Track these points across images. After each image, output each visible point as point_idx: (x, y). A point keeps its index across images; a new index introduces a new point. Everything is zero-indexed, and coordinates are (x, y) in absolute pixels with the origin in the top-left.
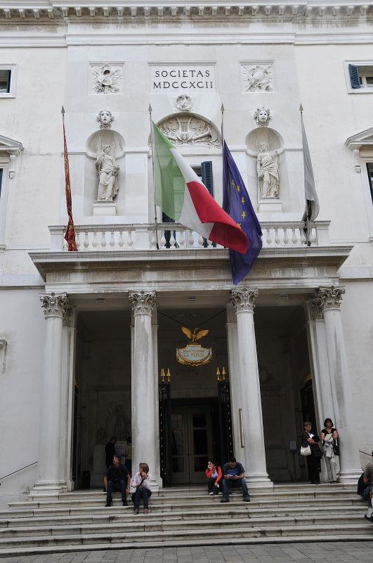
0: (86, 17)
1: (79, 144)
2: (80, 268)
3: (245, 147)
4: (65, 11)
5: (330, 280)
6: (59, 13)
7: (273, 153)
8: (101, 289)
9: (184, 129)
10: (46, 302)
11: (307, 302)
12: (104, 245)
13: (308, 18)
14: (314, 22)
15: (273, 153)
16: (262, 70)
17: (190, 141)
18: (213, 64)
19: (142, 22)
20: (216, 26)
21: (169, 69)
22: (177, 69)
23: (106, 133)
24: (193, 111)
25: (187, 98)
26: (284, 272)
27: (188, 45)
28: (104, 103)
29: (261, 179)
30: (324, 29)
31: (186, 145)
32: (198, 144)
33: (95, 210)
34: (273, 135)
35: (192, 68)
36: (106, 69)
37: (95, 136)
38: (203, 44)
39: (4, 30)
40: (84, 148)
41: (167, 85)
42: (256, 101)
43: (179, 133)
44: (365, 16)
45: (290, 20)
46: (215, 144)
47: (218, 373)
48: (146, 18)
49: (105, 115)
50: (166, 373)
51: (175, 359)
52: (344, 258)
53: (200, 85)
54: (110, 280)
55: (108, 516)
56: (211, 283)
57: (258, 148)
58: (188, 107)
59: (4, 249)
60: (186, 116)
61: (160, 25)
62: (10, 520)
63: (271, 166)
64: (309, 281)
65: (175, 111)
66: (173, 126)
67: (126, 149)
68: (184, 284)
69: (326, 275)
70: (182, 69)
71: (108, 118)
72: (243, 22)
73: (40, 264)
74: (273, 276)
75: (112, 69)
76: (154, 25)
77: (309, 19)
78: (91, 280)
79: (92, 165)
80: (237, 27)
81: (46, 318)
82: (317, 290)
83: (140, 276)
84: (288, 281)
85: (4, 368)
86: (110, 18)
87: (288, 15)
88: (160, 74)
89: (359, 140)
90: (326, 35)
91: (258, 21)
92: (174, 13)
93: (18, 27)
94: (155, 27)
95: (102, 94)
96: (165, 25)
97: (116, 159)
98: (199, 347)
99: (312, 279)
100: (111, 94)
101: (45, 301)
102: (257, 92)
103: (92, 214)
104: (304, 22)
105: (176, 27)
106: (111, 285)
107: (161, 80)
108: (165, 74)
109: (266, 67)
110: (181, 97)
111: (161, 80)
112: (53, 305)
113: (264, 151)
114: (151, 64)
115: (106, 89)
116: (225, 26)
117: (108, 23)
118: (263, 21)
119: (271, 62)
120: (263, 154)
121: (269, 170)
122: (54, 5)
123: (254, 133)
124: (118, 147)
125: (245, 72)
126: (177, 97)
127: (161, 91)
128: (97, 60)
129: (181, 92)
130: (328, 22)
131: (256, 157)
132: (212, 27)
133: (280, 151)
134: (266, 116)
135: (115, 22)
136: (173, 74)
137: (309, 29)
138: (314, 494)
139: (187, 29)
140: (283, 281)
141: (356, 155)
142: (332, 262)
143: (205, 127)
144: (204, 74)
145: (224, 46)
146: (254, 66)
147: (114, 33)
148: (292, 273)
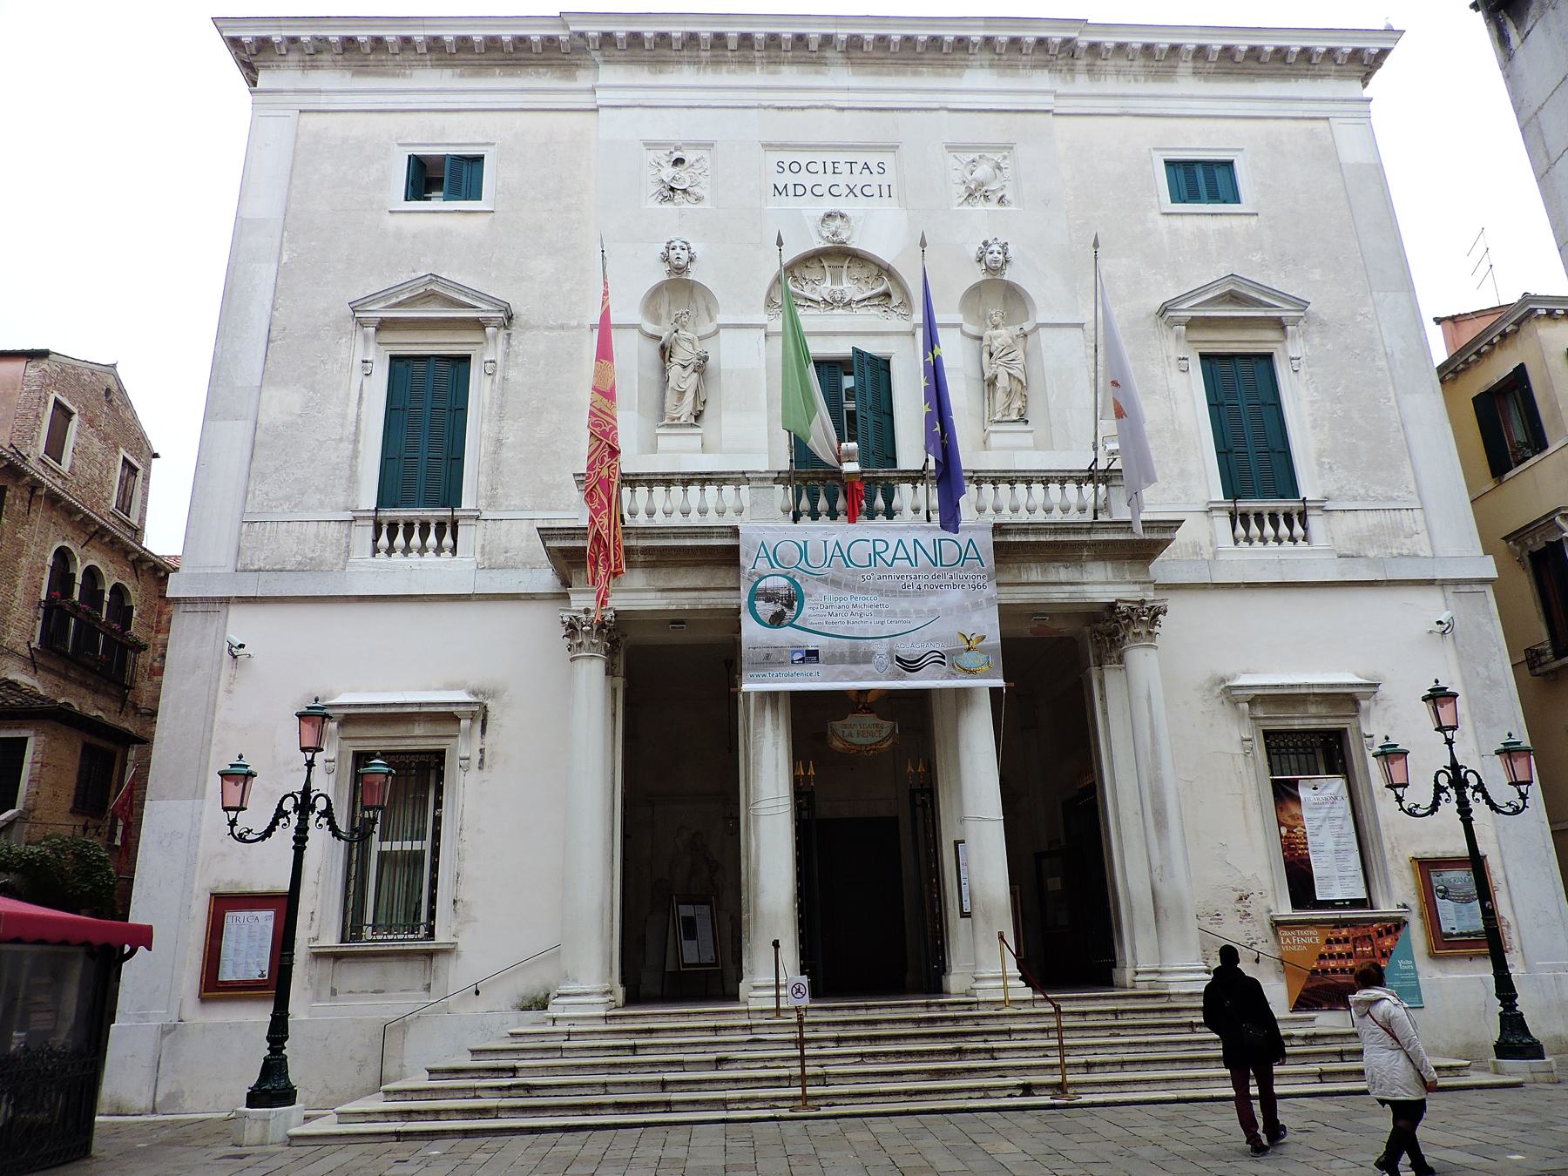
0: (638, 51)
1: (627, 310)
2: (641, 558)
3: (958, 318)
4: (594, 40)
5: (1137, 587)
6: (581, 42)
7: (1015, 330)
8: (684, 601)
9: (836, 279)
10: (572, 629)
11: (1087, 630)
12: (685, 513)
14: (1091, 71)
15: (1015, 330)
16: (992, 163)
17: (849, 304)
18: (893, 148)
19: (748, 62)
20: (897, 73)
21: (803, 158)
22: (820, 157)
23: (679, 286)
24: (854, 244)
25: (842, 216)
26: (1045, 571)
27: (843, 109)
28: (673, 222)
29: (992, 383)
30: (1110, 85)
31: (840, 311)
32: (864, 311)
33: (662, 442)
34: (1014, 297)
35: (851, 157)
36: (677, 155)
37: (656, 291)
38: (872, 109)
39: (470, 76)
40: (636, 317)
41: (800, 190)
42: (979, 225)
43: (826, 288)
44: (1190, 64)
45: (1043, 65)
46: (899, 310)
47: (910, 769)
49: (678, 250)
50: (806, 771)
51: (822, 737)
52: (1164, 544)
53: (867, 191)
54: (699, 583)
55: (714, 1057)
57: (983, 319)
58: (844, 236)
59: (477, 518)
60: (840, 255)
61: (785, 69)
62: (518, 1064)
63: (1011, 356)
64: (1098, 588)
65: (819, 244)
66: (813, 273)
67: (721, 319)
69: (1128, 578)
70: (829, 157)
71: (684, 255)
72: (951, 66)
73: (561, 550)
74: (1024, 578)
75: (690, 157)
76: (772, 67)
77: (1081, 63)
78: (661, 584)
79: (652, 349)
80: (938, 75)
81: (572, 660)
82: (1112, 606)
84: (1051, 589)
85: (482, 760)
86: (685, 53)
87: (1040, 56)
88: (786, 166)
89: (1185, 306)
90: (1115, 96)
91: (982, 66)
92: (814, 46)
93: (497, 71)
94: (775, 73)
95: (668, 206)
96: (794, 68)
97: (700, 339)
98: (870, 719)
99: (1101, 585)
100: (686, 206)
101: (571, 626)
102: (980, 207)
103: (654, 449)
104: (1071, 70)
105: (817, 73)
106: (704, 594)
107: (788, 179)
108: (795, 167)
109: (998, 157)
110: (829, 216)
111: (788, 179)
112: (587, 633)
113: (996, 327)
114: (768, 146)
115: (679, 196)
116: (915, 73)
117: (679, 62)
118: (991, 66)
119: (1009, 147)
120: (996, 332)
121: (1007, 365)
122: (572, 28)
123: (976, 290)
124: (704, 314)
125: (956, 166)
126: (822, 214)
127: (789, 203)
128: (659, 137)
129: (829, 205)
130: (1118, 72)
131: (981, 339)
132: (889, 74)
133: (1027, 327)
134: (1001, 257)
135: (695, 62)
136: (812, 167)
137: (1082, 83)
138: (1115, 1013)
139: (840, 80)
140: (1044, 589)
141: (1178, 337)
142: (1141, 549)
143: (879, 276)
144: (875, 169)
145: (915, 113)
146: (975, 156)
147: (692, 82)
148: (1063, 574)
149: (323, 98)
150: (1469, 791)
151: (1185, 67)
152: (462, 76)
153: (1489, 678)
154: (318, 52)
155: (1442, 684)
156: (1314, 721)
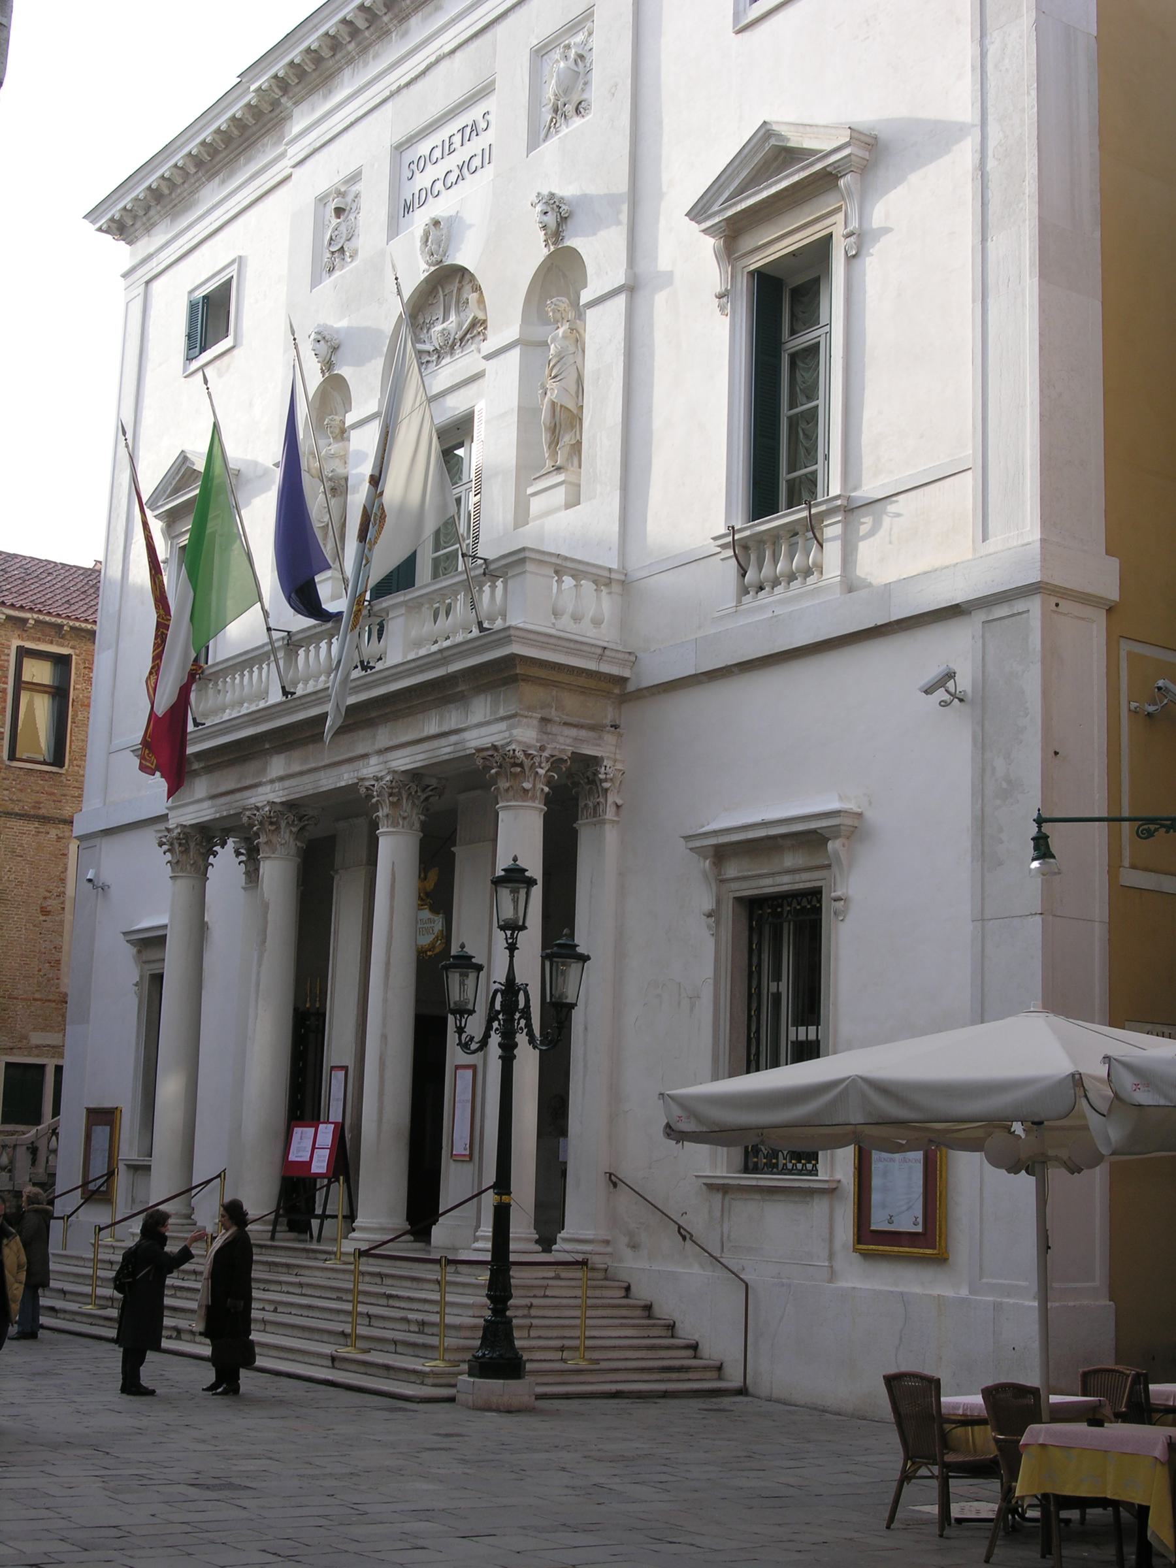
2: (196, 766)
5: (503, 726)
27: (453, 52)
48: (386, 19)
56: (344, 768)
61: (414, 21)
64: (484, 731)
68: (306, 779)
83: (264, 770)
89: (715, 208)
135: (350, 61)
149: (154, 262)
150: (517, 1016)
152: (223, 182)
154: (148, 209)
155: (521, 863)
156: (786, 879)
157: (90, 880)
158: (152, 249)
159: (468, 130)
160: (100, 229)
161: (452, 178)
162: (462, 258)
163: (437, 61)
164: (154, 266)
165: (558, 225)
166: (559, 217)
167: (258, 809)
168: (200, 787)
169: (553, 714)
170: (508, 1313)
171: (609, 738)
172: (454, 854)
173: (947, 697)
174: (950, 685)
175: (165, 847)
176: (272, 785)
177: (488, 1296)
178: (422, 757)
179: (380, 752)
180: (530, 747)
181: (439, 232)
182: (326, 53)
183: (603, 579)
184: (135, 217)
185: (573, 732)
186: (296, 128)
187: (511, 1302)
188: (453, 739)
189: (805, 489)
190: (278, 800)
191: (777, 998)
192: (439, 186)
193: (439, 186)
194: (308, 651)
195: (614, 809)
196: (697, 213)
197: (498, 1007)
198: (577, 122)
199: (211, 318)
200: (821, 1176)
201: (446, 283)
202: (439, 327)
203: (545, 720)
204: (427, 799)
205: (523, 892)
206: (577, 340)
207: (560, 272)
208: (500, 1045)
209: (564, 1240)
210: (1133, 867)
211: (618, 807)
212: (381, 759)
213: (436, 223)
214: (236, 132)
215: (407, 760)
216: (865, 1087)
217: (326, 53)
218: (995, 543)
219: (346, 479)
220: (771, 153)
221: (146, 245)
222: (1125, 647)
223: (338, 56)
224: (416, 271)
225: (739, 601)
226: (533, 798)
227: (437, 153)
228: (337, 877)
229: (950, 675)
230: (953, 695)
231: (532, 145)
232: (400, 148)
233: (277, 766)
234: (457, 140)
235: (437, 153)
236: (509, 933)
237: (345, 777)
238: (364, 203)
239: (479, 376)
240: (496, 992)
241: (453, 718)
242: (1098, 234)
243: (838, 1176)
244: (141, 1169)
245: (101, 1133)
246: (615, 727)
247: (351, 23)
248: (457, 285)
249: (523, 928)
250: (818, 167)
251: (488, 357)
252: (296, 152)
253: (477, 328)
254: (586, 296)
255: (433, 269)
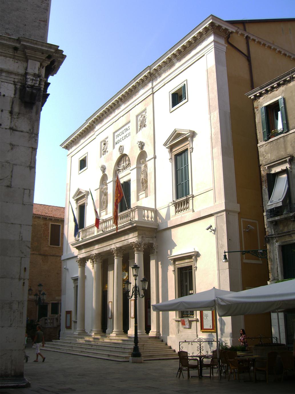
13: (156, 75)
26: (124, 238)
27: (123, 116)
56: (108, 246)
64: (132, 239)
84: (125, 241)
89: (168, 144)
91: (141, 88)
150: (137, 292)
151: (175, 60)
152: (84, 139)
153: (222, 245)
154: (71, 144)
156: (186, 264)
157: (65, 268)
158: (72, 151)
159: (126, 130)
160: (63, 148)
161: (124, 138)
162: (124, 152)
163: (120, 118)
164: (73, 154)
165: (142, 147)
166: (142, 145)
167: (93, 254)
168: (83, 251)
169: (144, 236)
170: (138, 345)
171: (155, 239)
172: (129, 261)
173: (211, 230)
174: (211, 228)
175: (77, 262)
176: (96, 250)
177: (134, 342)
178: (121, 244)
179: (114, 243)
180: (140, 242)
181: (121, 148)
182: (101, 116)
183: (152, 210)
184: (69, 145)
185: (148, 239)
186: (95, 130)
187: (138, 344)
188: (127, 241)
189: (187, 193)
190: (97, 253)
191: (186, 286)
192: (121, 140)
193: (121, 140)
194: (101, 225)
195: (156, 253)
196: (165, 145)
197: (134, 290)
198: (144, 128)
199: (83, 164)
200: (195, 318)
201: (123, 157)
202: (122, 165)
203: (142, 237)
204: (123, 252)
205: (137, 269)
206: (146, 166)
207: (143, 155)
208: (134, 297)
209: (151, 332)
210: (245, 259)
211: (157, 252)
212: (114, 245)
213: (121, 146)
214: (86, 130)
215: (119, 245)
216: (184, 303)
217: (101, 116)
218: (217, 203)
219: (107, 193)
220: (176, 135)
221: (71, 150)
222: (242, 220)
223: (103, 117)
224: (117, 155)
225: (176, 214)
226: (141, 251)
227: (121, 134)
228: (109, 266)
229: (211, 226)
230: (212, 230)
231: (137, 132)
232: (114, 133)
233: (97, 247)
234: (124, 131)
235: (121, 134)
236: (135, 277)
237: (108, 248)
238: (108, 142)
239: (130, 173)
240: (133, 288)
241: (126, 237)
242: (232, 147)
243: (197, 318)
244: (76, 322)
245: (69, 315)
246: (155, 237)
247: (105, 111)
248: (125, 157)
249: (137, 276)
250: (185, 136)
251: (131, 170)
252: (97, 133)
253: (129, 164)
254: (147, 159)
255: (121, 155)
